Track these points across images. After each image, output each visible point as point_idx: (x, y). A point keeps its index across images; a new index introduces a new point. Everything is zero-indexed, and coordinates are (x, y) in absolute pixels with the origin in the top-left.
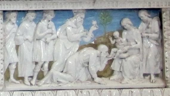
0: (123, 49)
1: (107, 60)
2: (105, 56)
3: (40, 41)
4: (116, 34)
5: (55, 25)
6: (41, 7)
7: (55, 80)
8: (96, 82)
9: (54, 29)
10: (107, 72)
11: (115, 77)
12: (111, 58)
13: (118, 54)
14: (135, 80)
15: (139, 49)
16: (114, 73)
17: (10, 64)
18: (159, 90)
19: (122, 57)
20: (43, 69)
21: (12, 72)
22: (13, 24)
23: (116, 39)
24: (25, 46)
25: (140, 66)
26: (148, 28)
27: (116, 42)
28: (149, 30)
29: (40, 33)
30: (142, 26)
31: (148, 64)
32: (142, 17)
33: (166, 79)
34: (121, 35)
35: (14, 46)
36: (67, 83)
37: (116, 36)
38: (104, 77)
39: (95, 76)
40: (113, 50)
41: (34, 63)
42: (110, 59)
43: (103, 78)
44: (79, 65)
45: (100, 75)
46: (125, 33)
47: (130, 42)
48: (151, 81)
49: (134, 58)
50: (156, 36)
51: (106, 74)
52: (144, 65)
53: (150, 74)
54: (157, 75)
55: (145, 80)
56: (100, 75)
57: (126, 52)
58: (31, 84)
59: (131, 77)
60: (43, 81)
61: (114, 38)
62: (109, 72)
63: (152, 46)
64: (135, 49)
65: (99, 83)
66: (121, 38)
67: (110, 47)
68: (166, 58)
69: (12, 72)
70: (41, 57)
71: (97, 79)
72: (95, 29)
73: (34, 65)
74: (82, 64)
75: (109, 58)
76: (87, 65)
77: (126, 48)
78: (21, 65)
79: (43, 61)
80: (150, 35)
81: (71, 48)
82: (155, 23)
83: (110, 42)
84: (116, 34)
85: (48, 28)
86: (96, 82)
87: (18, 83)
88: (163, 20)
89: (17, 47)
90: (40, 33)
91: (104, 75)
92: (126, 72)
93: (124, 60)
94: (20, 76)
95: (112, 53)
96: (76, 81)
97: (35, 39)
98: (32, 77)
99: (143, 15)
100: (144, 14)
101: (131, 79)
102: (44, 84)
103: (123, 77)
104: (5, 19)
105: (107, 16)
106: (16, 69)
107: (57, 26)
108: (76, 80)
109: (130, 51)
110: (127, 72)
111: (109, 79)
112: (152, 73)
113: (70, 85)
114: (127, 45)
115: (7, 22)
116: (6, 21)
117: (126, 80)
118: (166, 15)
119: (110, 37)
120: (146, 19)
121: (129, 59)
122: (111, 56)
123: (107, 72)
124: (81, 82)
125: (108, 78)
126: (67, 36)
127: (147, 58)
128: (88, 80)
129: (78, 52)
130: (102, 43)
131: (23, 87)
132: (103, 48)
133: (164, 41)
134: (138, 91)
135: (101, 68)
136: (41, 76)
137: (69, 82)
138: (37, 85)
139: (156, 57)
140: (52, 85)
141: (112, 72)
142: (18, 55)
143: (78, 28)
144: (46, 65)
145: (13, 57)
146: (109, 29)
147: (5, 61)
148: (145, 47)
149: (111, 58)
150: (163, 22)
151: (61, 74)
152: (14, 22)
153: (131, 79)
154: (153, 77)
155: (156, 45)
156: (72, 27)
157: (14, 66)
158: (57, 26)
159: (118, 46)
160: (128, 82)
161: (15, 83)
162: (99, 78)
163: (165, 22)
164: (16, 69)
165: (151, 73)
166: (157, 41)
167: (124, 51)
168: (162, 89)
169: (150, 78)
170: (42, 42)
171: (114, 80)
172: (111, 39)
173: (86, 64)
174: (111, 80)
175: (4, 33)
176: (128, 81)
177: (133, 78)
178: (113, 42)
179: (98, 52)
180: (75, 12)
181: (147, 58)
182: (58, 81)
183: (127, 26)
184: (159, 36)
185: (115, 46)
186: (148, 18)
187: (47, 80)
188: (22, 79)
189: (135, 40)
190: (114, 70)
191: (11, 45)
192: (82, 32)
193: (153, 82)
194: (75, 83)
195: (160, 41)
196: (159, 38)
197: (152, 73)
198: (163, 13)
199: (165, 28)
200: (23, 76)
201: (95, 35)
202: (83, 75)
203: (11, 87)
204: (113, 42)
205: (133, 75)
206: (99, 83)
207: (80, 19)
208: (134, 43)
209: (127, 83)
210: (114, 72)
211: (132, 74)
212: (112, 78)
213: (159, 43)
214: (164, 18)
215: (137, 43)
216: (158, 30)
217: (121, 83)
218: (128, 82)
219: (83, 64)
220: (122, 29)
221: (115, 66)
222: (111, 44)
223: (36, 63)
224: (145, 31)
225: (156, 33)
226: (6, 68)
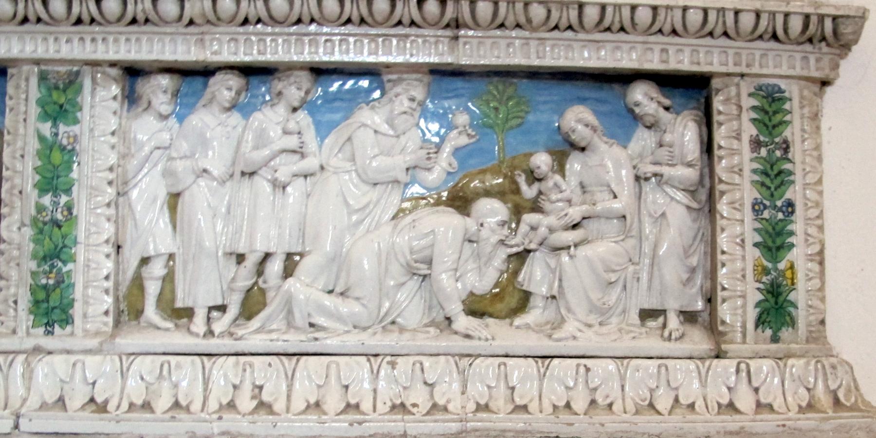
0: (563, 213)
1: (503, 253)
2: (494, 239)
3: (256, 178)
4: (542, 161)
5: (318, 125)
6: (255, 52)
7: (300, 320)
8: (456, 333)
9: (310, 137)
10: (504, 301)
11: (533, 316)
12: (517, 245)
13: (543, 230)
14: (604, 329)
15: (624, 217)
16: (533, 301)
17: (145, 261)
18: (692, 365)
19: (559, 245)
20: (265, 282)
21: (152, 289)
22: (164, 117)
23: (540, 180)
24: (201, 198)
25: (628, 280)
26: (661, 146)
27: (540, 193)
28: (663, 153)
29: (256, 148)
30: (643, 139)
31: (656, 273)
32: (637, 104)
33: (721, 328)
34: (561, 169)
35: (162, 195)
36: (348, 332)
37: (539, 168)
38: (491, 316)
39: (455, 308)
40: (529, 218)
41: (234, 258)
42: (515, 250)
43: (490, 321)
44: (396, 269)
45: (476, 308)
46: (575, 164)
47: (593, 195)
48: (666, 334)
49: (603, 249)
50: (691, 174)
51: (500, 307)
52: (645, 277)
53: (663, 312)
54: (689, 317)
55: (643, 330)
56: (476, 308)
57: (575, 226)
58: (210, 333)
59: (593, 319)
60: (256, 323)
61: (533, 177)
62: (512, 301)
63: (673, 209)
64: (608, 216)
65: (468, 336)
66: (558, 178)
67: (517, 212)
68: (723, 252)
69: (152, 289)
70: (251, 237)
71: (463, 322)
72: (464, 140)
73: (233, 267)
74: (405, 264)
75: (512, 247)
76: (421, 270)
77: (575, 213)
78: (185, 263)
79: (261, 247)
80: (665, 170)
81: (367, 205)
82: (685, 133)
83: (517, 191)
84: (542, 161)
85: (286, 132)
86: (456, 333)
87: (167, 330)
88: (716, 118)
89: (174, 199)
90: (256, 148)
91: (490, 310)
92: (570, 296)
93: (565, 258)
94: (179, 304)
95: (524, 228)
96: (383, 327)
97: (238, 174)
98: (222, 308)
99: (642, 95)
100: (646, 94)
101: (590, 326)
102: (258, 331)
103: (562, 317)
104: (131, 98)
105: (509, 99)
106: (169, 279)
107: (323, 130)
108: (381, 321)
109: (592, 226)
110: (573, 297)
111: (511, 324)
112: (673, 305)
113: (353, 341)
114: (584, 203)
115: (140, 109)
116: (138, 107)
117: (571, 327)
118: (727, 101)
119: (520, 175)
120: (651, 112)
121: (583, 252)
122: (518, 243)
123: (504, 301)
124: (402, 330)
125: (508, 321)
126: (355, 164)
127: (654, 256)
128: (432, 323)
129: (393, 222)
130: (488, 193)
131: (180, 340)
132: (491, 211)
133: (717, 193)
134: (611, 365)
135: (483, 280)
136: (252, 304)
137: (355, 327)
138: (231, 334)
139: (687, 253)
140: (285, 337)
141: (526, 297)
142: (174, 227)
143: (398, 137)
144: (275, 267)
145: (155, 234)
146: (516, 144)
147: (126, 251)
148: (650, 215)
149: (517, 245)
150: (715, 126)
151: (329, 301)
152: (165, 109)
153: (590, 326)
154: (674, 322)
155: (688, 208)
156: (376, 132)
157: (157, 269)
158: (323, 130)
159: (547, 206)
160: (579, 334)
161: (158, 328)
162: (470, 318)
163: (720, 124)
164: (169, 279)
165: (666, 307)
166: (692, 193)
167: (568, 221)
168: (703, 364)
169: (664, 326)
170: (261, 184)
171: (528, 326)
172: (522, 180)
173: (425, 266)
174: (518, 327)
175: (122, 149)
176: (580, 331)
177: (601, 324)
178: (528, 192)
179: (470, 223)
180: (389, 81)
181: (654, 256)
182: (312, 325)
183: (581, 134)
184: (702, 176)
185: (536, 207)
186: (661, 110)
187: (269, 318)
188: (189, 313)
189: (609, 186)
190: (531, 289)
191: (147, 192)
192: (413, 152)
193: (673, 337)
194: (375, 333)
195: (703, 195)
196: (701, 182)
197: (673, 305)
198: (716, 94)
199: (720, 147)
200: (190, 304)
201: (462, 163)
202: (410, 305)
203: (132, 340)
204: (528, 192)
205: (603, 313)
206: (468, 336)
207: (407, 103)
208: (607, 196)
209: (575, 338)
210: (532, 299)
211: (593, 309)
212: (518, 321)
213: (699, 202)
214: (720, 113)
215: (615, 197)
216: (697, 154)
217: (550, 336)
218: (576, 334)
219: (408, 264)
220: (566, 148)
221: (536, 276)
222: (522, 198)
223: (240, 258)
224: (650, 159)
225: (690, 165)
226: (130, 273)
